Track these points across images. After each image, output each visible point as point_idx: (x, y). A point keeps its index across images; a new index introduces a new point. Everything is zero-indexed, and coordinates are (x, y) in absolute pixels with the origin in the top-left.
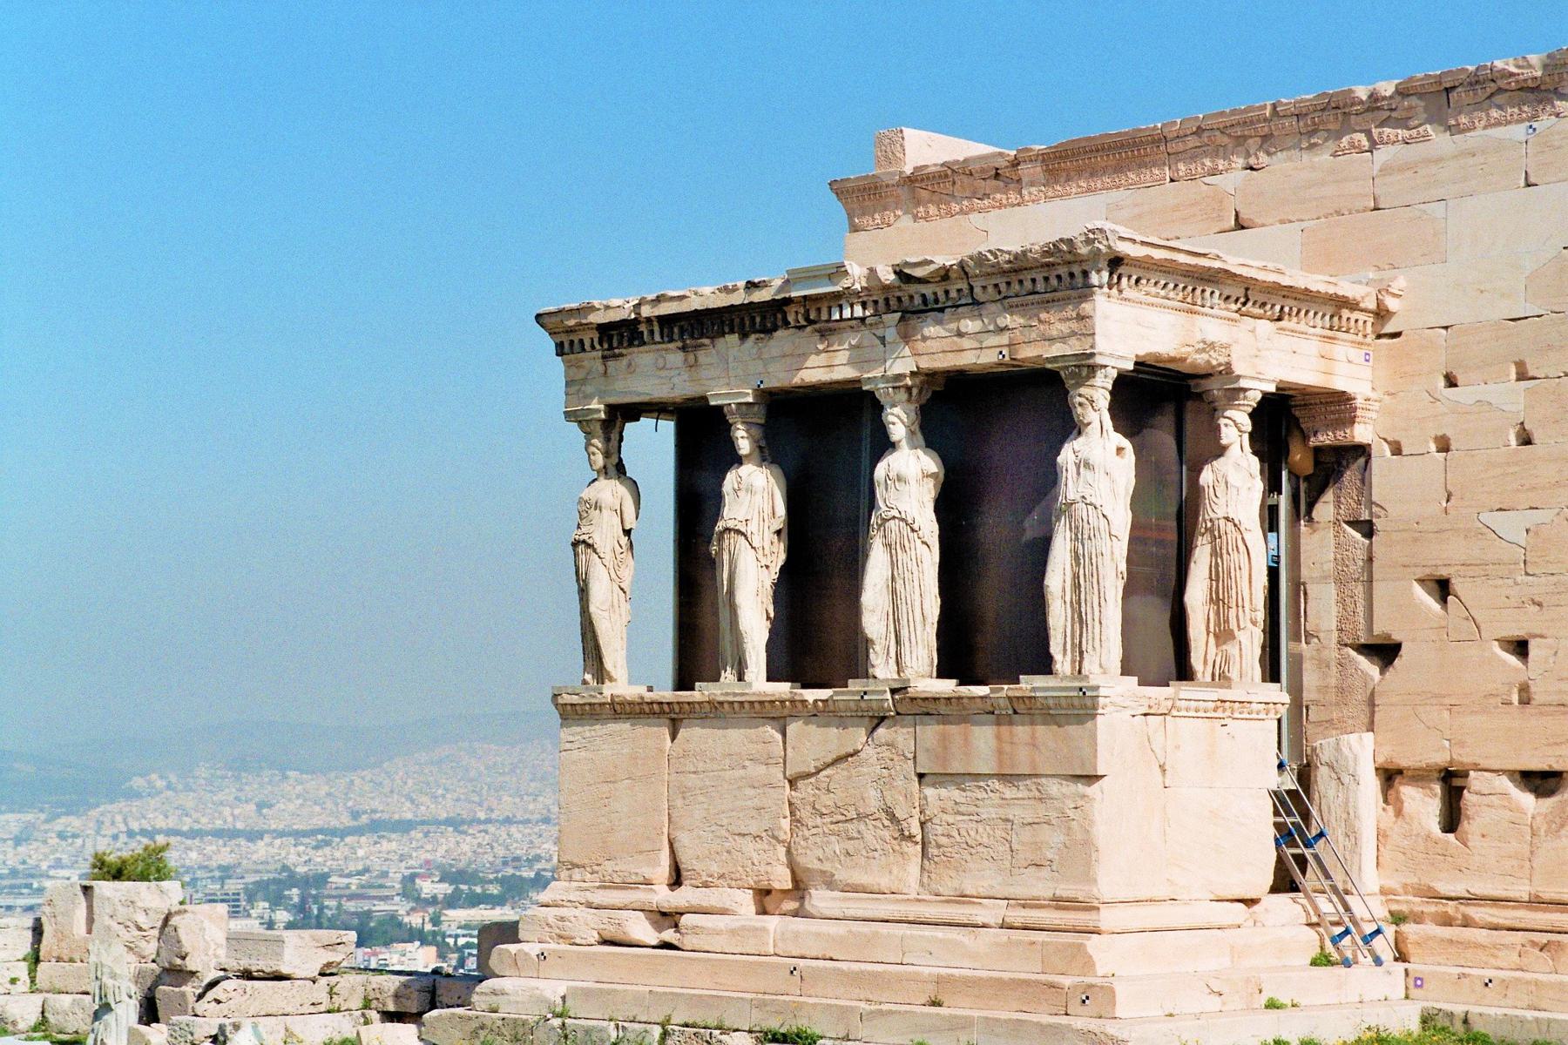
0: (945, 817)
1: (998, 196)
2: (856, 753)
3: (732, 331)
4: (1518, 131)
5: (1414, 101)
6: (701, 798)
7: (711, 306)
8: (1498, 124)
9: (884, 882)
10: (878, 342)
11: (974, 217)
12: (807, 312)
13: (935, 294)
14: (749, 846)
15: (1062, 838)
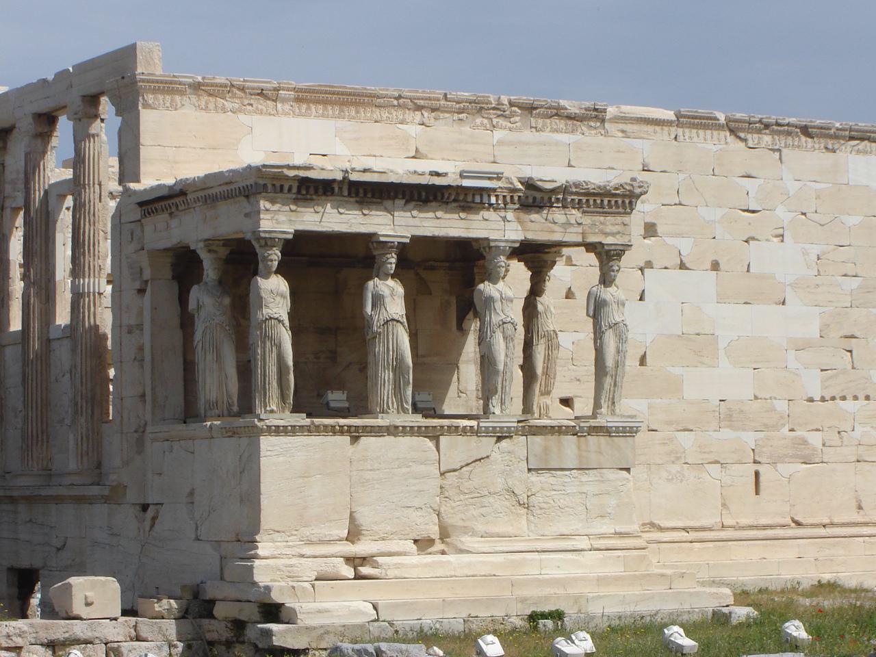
0: (544, 492)
1: (260, 106)
2: (488, 457)
3: (403, 198)
4: (565, 138)
5: (516, 109)
6: (377, 486)
7: (405, 181)
8: (556, 131)
9: (509, 529)
10: (501, 219)
11: (242, 117)
12: (458, 194)
13: (542, 198)
14: (414, 515)
15: (615, 501)
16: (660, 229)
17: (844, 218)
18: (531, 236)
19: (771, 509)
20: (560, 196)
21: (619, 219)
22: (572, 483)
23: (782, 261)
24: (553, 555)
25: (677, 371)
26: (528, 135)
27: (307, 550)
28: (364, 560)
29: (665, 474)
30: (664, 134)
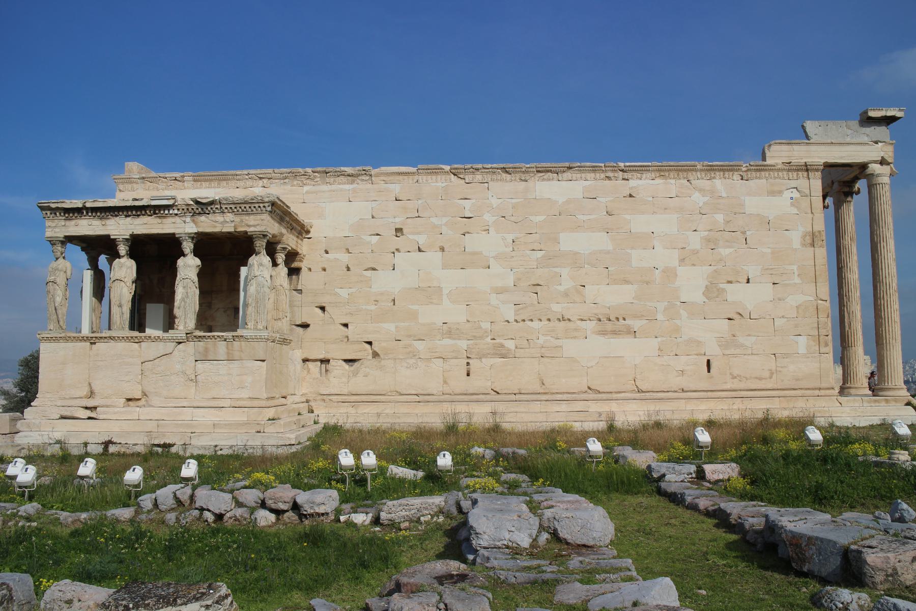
4: (347, 187)
16: (405, 231)
17: (532, 218)
18: (201, 230)
19: (477, 383)
20: (218, 207)
21: (259, 217)
22: (223, 367)
23: (487, 243)
24: (202, 410)
25: (415, 307)
26: (325, 188)
27: (59, 403)
28: (95, 408)
29: (406, 365)
30: (410, 180)
